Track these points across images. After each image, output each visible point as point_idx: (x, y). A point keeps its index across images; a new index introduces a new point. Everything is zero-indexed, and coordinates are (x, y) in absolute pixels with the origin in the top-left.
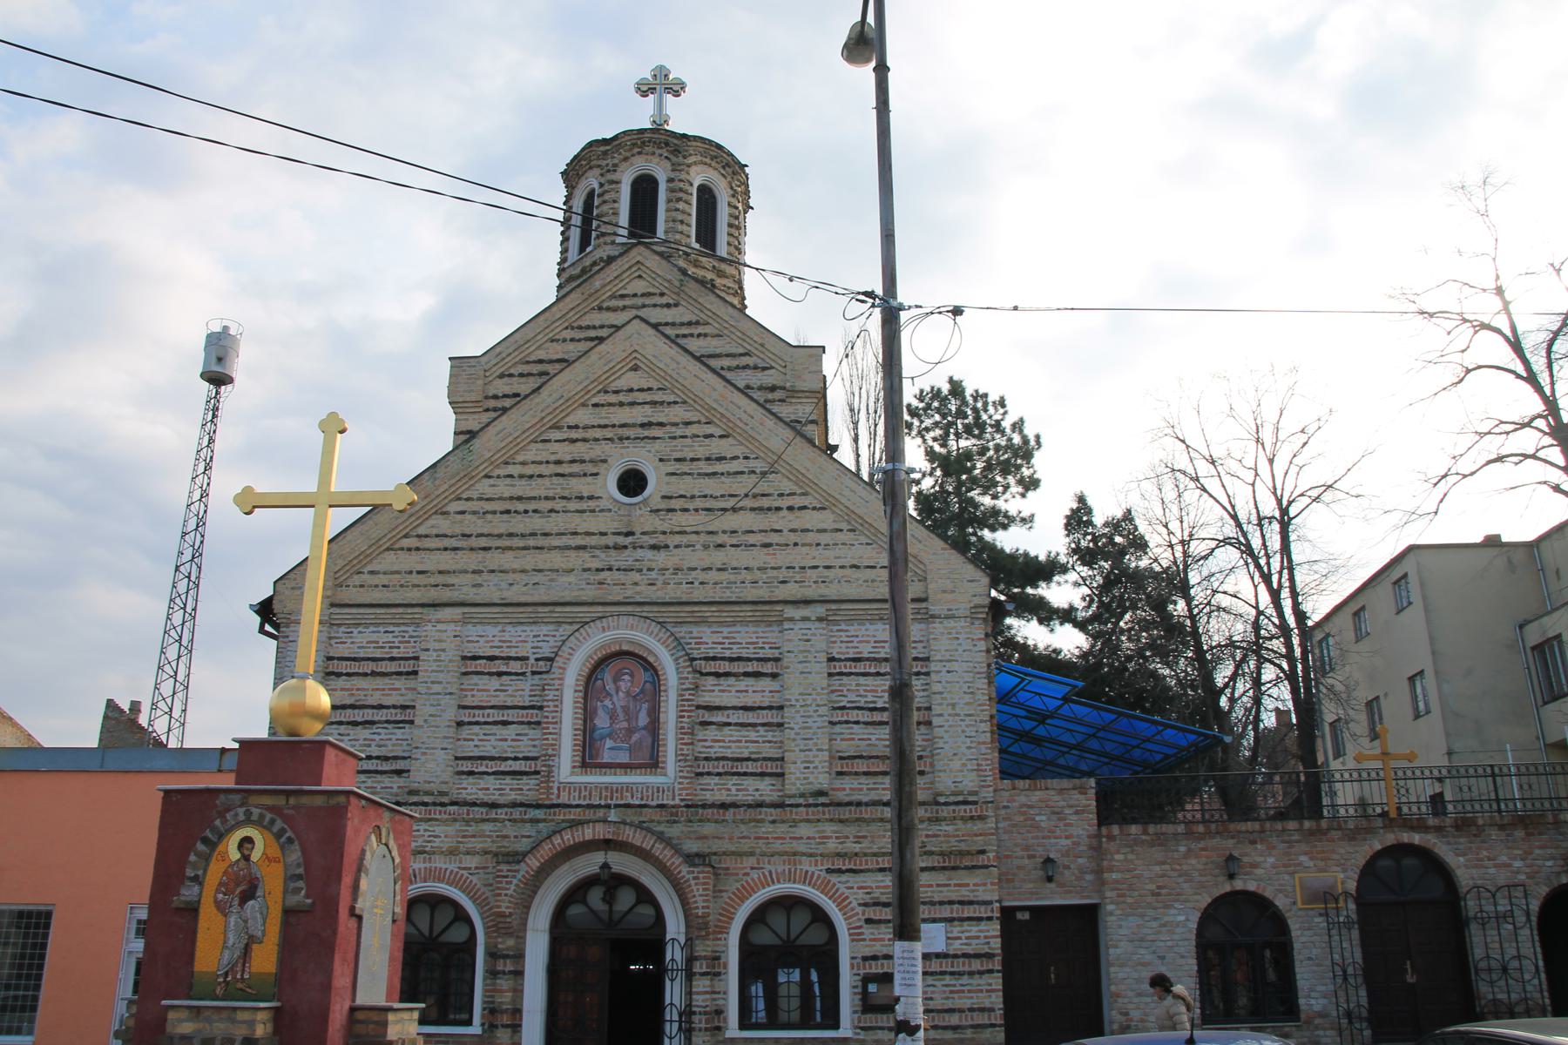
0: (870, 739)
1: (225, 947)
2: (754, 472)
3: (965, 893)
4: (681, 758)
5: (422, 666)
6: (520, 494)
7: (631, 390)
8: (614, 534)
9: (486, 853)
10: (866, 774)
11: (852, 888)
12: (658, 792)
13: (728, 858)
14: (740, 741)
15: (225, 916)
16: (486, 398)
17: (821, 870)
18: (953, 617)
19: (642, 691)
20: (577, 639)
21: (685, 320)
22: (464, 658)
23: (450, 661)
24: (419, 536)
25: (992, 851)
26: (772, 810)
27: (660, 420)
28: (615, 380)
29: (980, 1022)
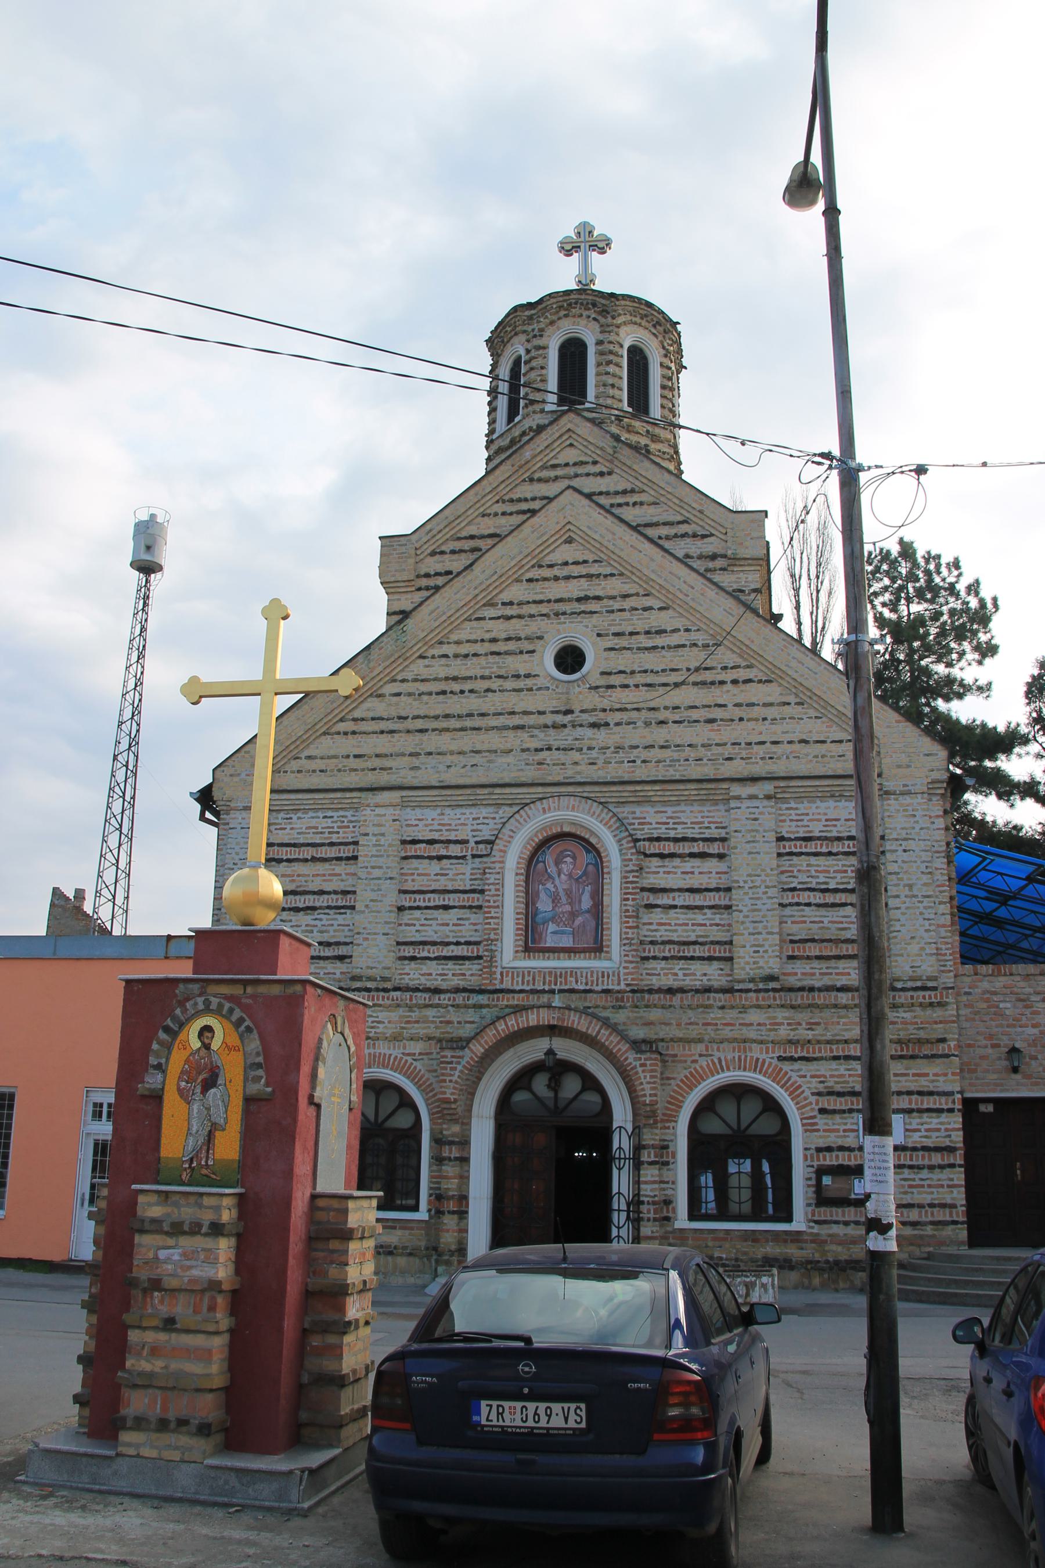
0: (822, 922)
1: (189, 1133)
2: (695, 645)
3: (924, 1084)
4: (626, 942)
5: (362, 851)
6: (456, 674)
7: (566, 564)
8: (553, 712)
9: (430, 1039)
10: (818, 958)
11: (805, 1076)
12: (603, 977)
13: (676, 1045)
14: (687, 925)
15: (189, 1103)
16: (418, 576)
17: (772, 1058)
18: (909, 793)
19: (585, 873)
20: (517, 820)
21: (620, 488)
22: (404, 842)
23: (390, 845)
24: (355, 720)
25: (953, 1039)
26: (721, 995)
27: (597, 594)
28: (549, 553)
29: (941, 1219)
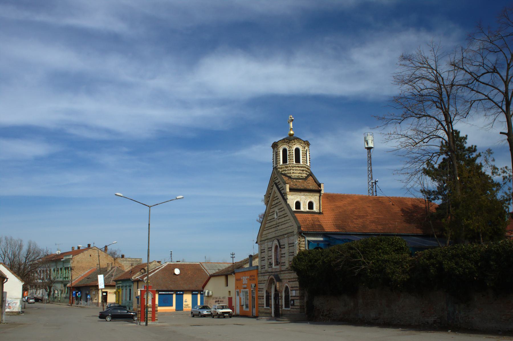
22: (269, 248)
